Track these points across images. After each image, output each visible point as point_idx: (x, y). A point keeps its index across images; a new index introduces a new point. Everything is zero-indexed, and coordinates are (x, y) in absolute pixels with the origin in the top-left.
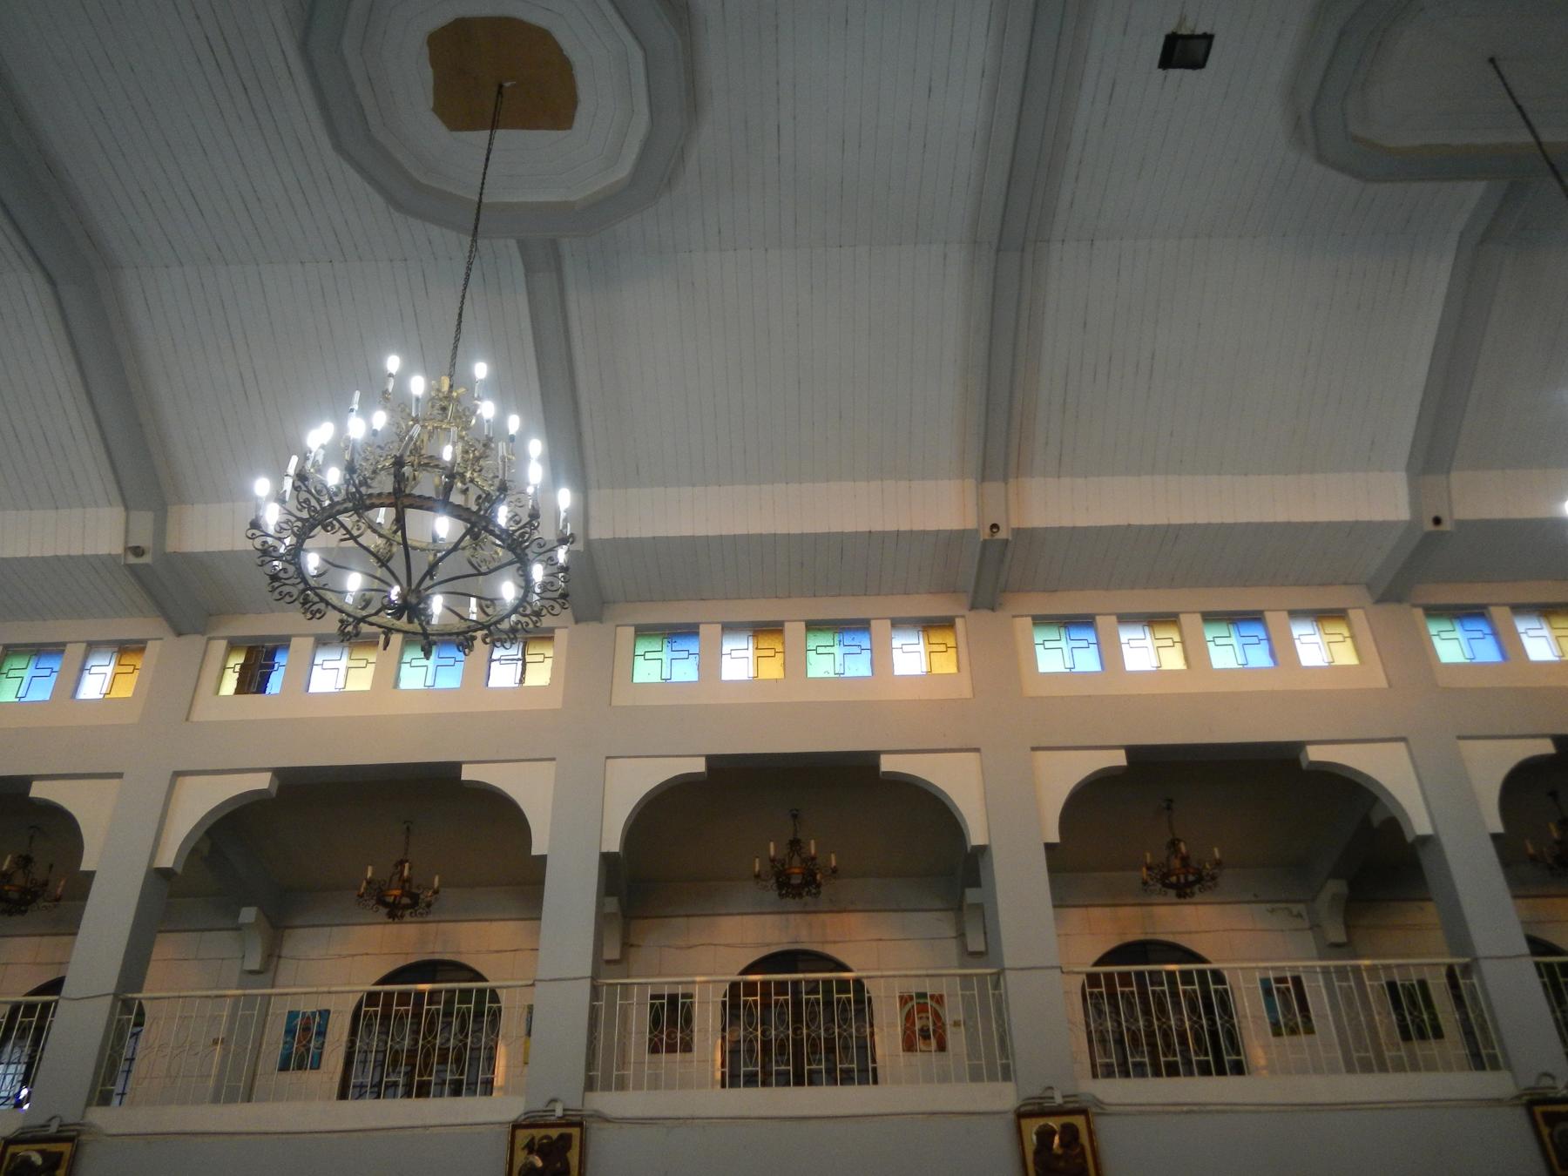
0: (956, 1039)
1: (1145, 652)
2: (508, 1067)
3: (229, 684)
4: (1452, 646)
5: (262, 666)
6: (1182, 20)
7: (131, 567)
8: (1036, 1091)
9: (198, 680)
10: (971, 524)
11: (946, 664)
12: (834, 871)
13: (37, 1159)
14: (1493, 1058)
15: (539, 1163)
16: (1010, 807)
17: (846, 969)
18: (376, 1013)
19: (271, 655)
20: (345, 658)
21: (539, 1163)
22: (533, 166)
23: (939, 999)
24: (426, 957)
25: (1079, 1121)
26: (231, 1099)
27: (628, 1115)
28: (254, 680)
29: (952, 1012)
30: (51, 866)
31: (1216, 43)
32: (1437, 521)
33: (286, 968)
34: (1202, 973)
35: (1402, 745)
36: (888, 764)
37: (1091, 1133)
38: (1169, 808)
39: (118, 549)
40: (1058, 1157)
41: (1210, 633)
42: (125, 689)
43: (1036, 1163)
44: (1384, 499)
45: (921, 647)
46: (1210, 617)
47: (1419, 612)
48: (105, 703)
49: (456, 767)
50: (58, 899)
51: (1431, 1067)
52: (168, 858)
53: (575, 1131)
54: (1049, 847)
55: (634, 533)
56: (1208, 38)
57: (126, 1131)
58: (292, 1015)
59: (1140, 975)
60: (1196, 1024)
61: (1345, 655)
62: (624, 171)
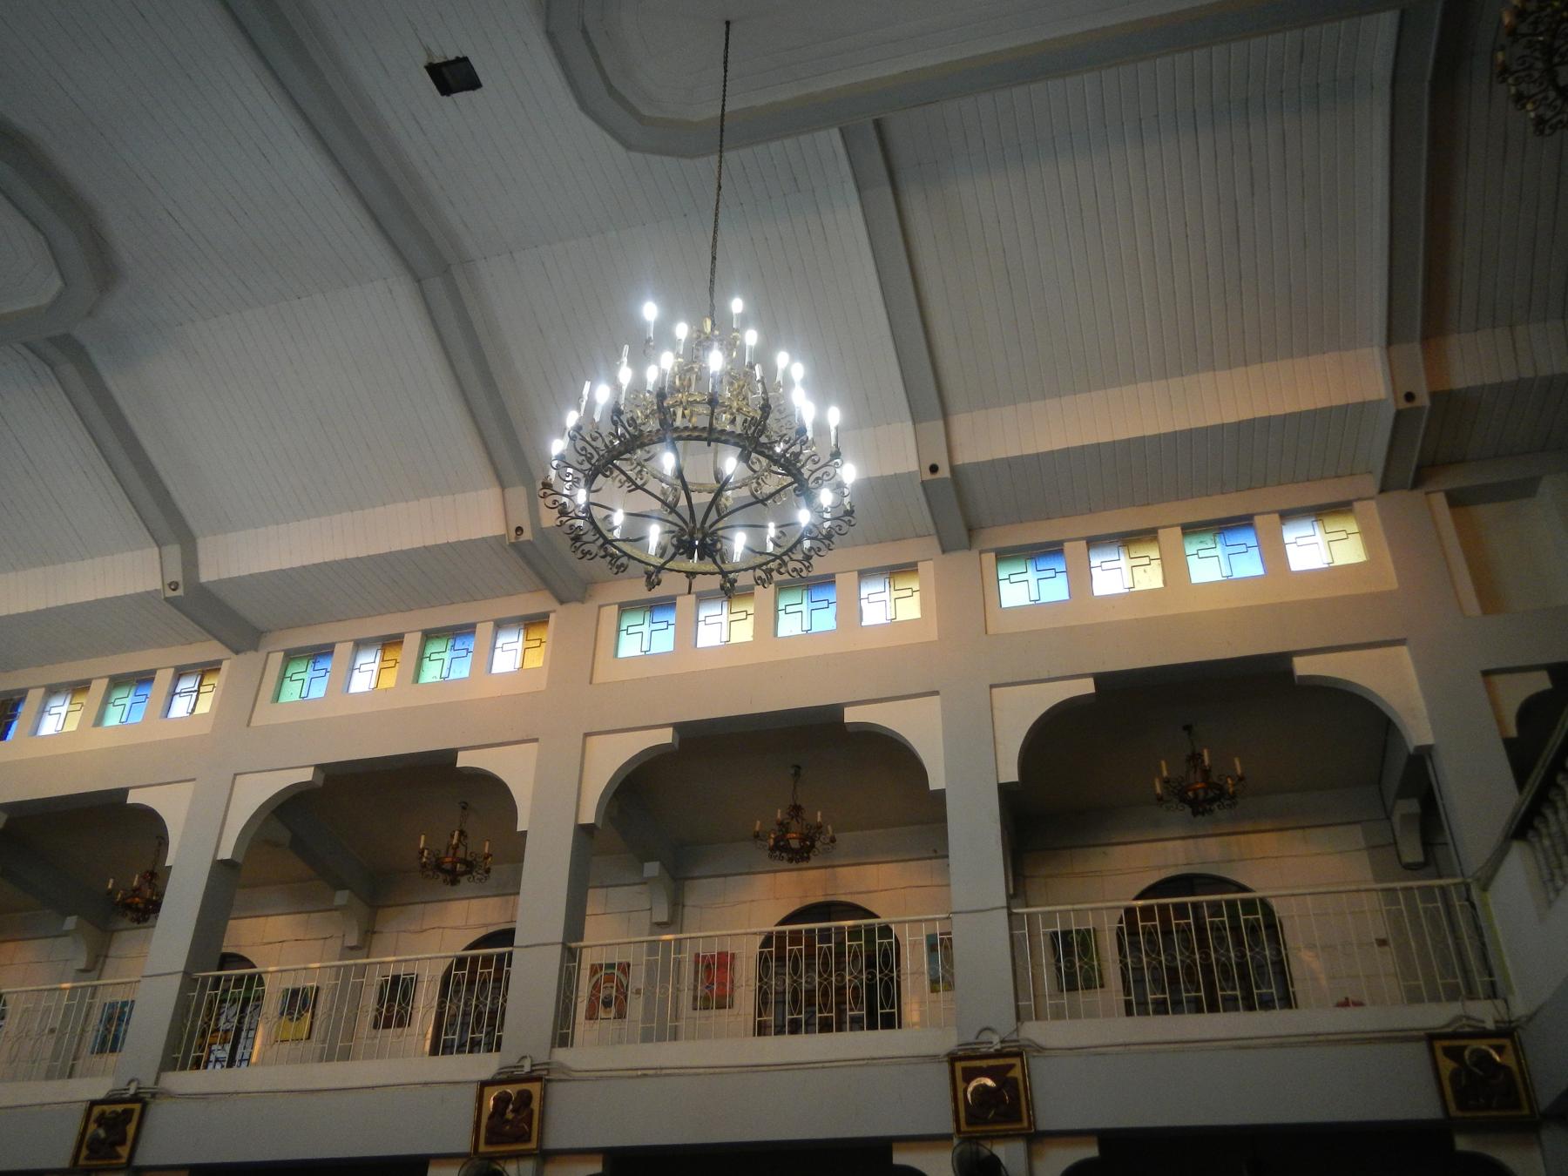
0: (635, 1007)
8: (512, 1060)
16: (551, 794)
21: (102, 1133)
23: (625, 968)
25: (535, 1088)
29: (637, 979)
36: (463, 760)
37: (543, 1098)
40: (508, 1121)
41: (1191, 547)
47: (989, 558)
49: (124, 792)
51: (1091, 1014)
53: (137, 1107)
54: (1004, 789)
55: (235, 574)
59: (1196, 906)
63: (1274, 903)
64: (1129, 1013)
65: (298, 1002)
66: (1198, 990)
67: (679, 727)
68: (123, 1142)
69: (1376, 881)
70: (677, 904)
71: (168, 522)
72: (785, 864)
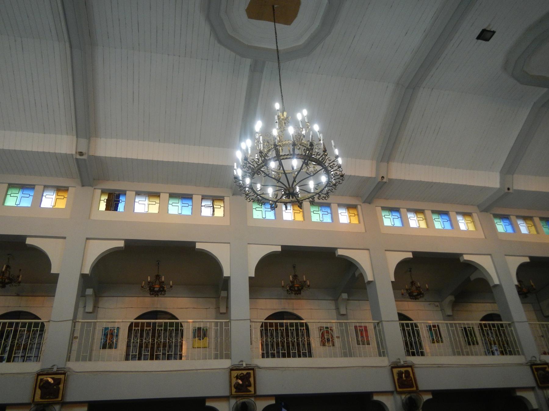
1: (415, 222)
2: (187, 349)
3: (103, 206)
4: (501, 227)
5: (115, 201)
6: (489, 25)
7: (77, 159)
9: (92, 204)
10: (374, 175)
11: (355, 220)
12: (309, 286)
13: (50, 380)
14: (518, 351)
15: (240, 382)
17: (302, 319)
18: (150, 330)
19: (118, 197)
20: (147, 200)
21: (240, 382)
22: (261, 33)
24: (155, 309)
25: (409, 369)
26: (84, 359)
27: (266, 366)
28: (112, 205)
30: (20, 270)
31: (495, 35)
32: (509, 189)
33: (101, 312)
34: (412, 324)
35: (489, 257)
37: (413, 373)
38: (410, 271)
39: (74, 153)
42: (62, 204)
43: (398, 382)
44: (492, 181)
45: (347, 214)
46: (434, 212)
47: (492, 216)
48: (53, 210)
49: (194, 243)
50: (20, 282)
52: (87, 270)
53: (251, 372)
56: (494, 32)
57: (143, 370)
58: (106, 329)
60: (455, 339)
61: (471, 228)
62: (302, 42)
63: (309, 324)
64: (263, 357)
65: (200, 333)
66: (274, 351)
67: (414, 253)
68: (250, 386)
69: (538, 321)
70: (96, 307)
71: (86, 125)
72: (410, 300)
